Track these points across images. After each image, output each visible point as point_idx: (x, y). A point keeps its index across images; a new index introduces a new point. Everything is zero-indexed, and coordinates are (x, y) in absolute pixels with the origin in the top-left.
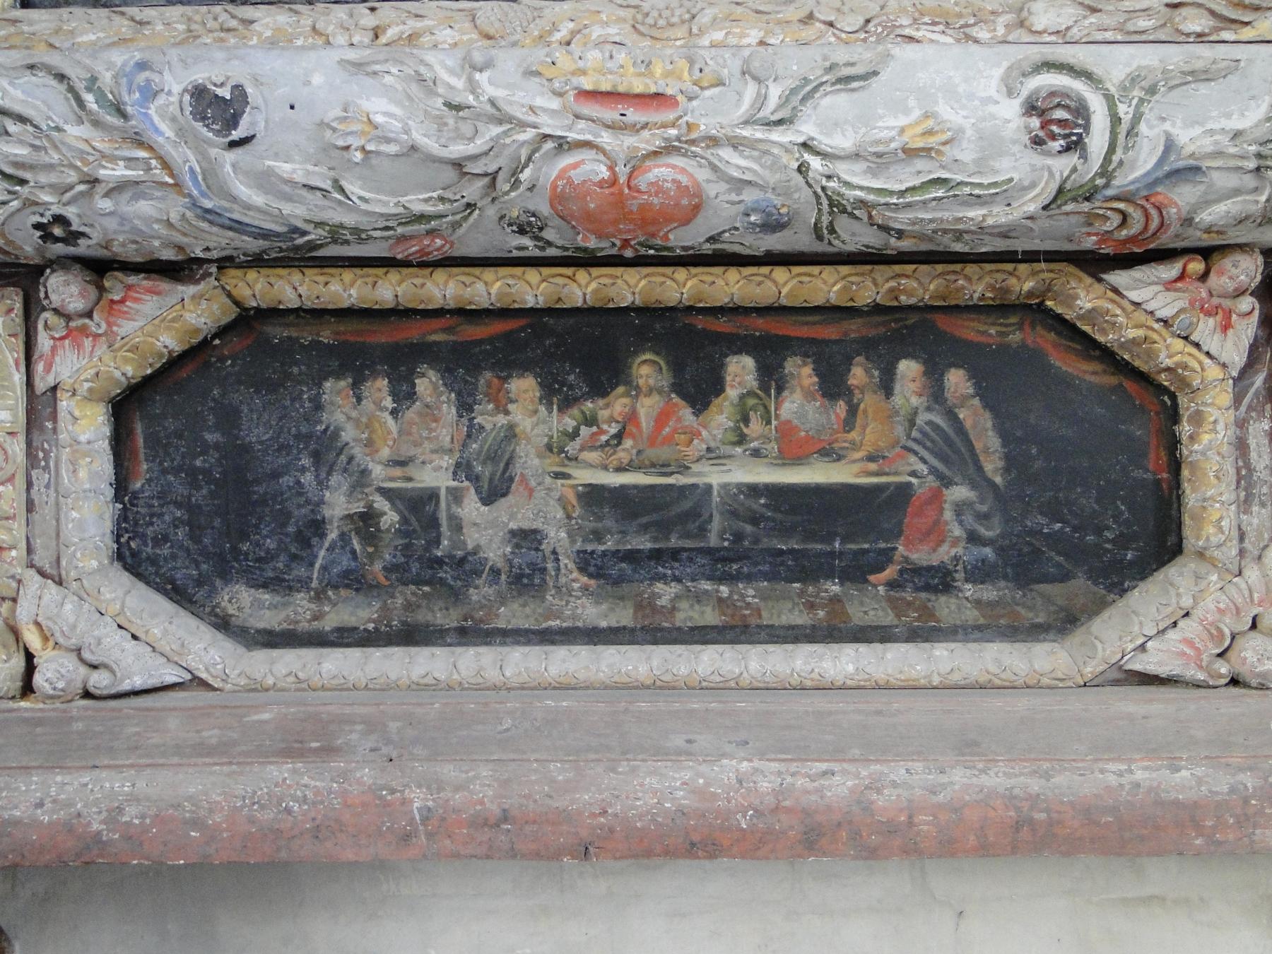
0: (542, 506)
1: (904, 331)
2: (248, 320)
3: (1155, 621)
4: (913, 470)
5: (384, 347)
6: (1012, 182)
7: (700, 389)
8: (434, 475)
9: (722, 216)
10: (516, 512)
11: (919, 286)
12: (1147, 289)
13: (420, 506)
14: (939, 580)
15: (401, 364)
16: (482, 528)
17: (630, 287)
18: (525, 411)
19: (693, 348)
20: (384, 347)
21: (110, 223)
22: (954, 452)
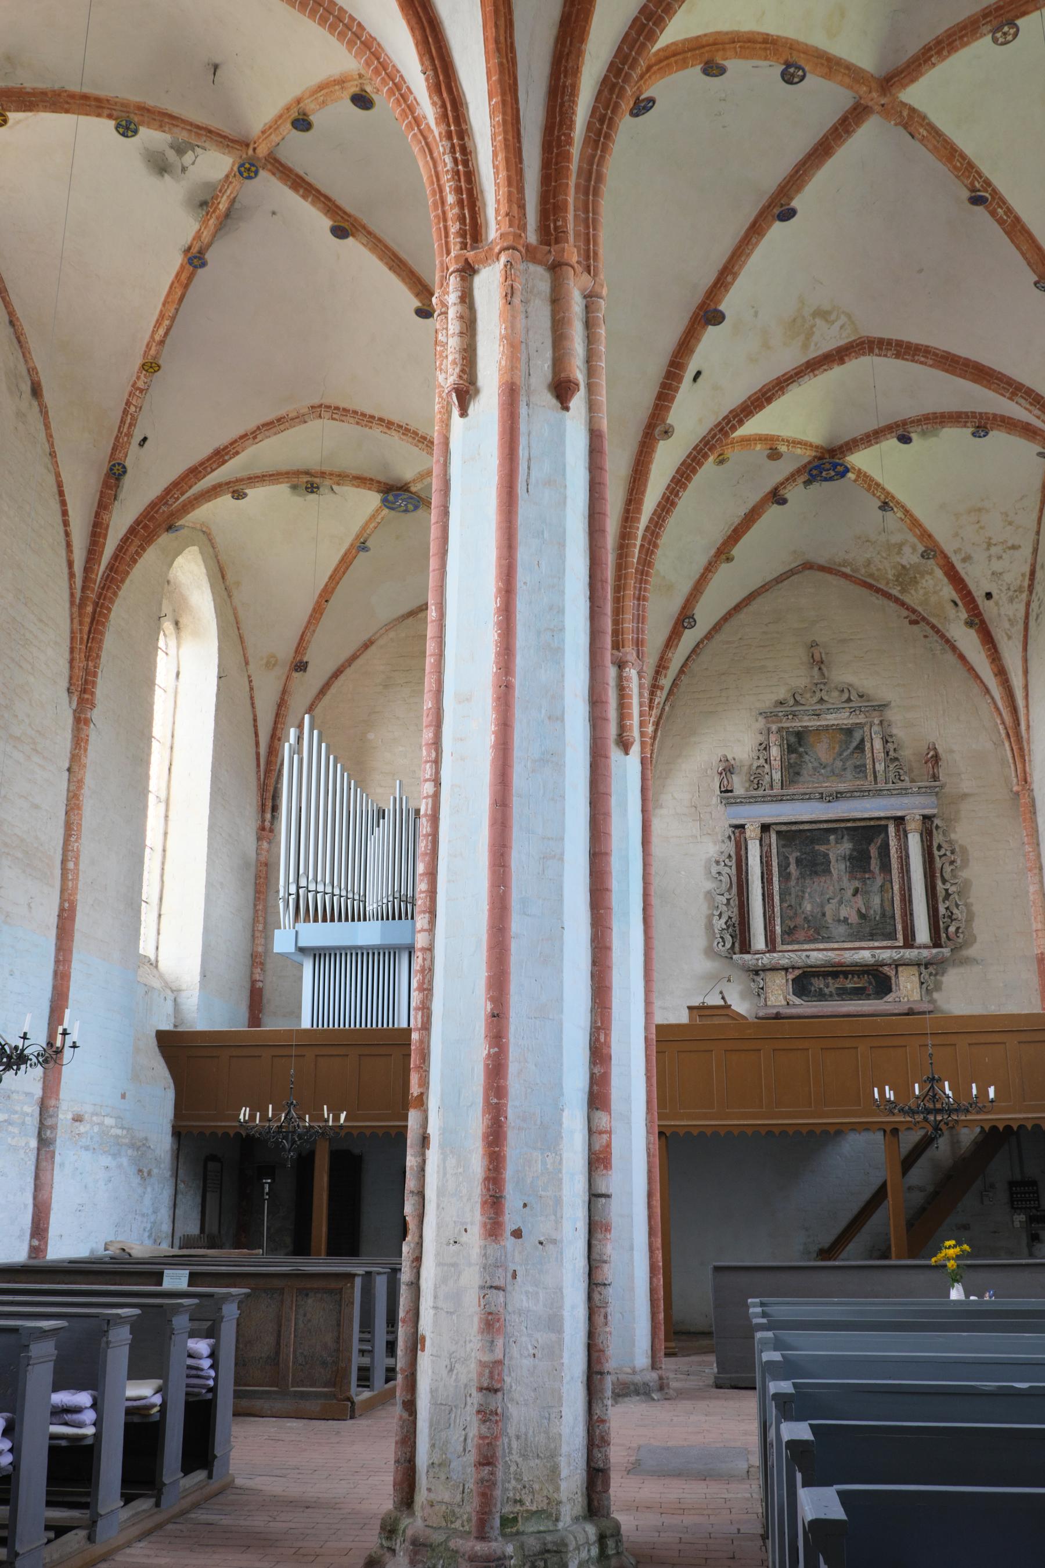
0: (832, 989)
1: (864, 972)
2: (804, 972)
3: (889, 998)
4: (867, 985)
5: (817, 974)
6: (872, 961)
7: (847, 978)
8: (822, 986)
9: (848, 963)
10: (830, 989)
11: (865, 968)
12: (886, 968)
13: (821, 989)
14: (870, 995)
15: (818, 977)
16: (826, 991)
17: (839, 969)
18: (830, 980)
19: (846, 974)
20: (817, 974)
21: (796, 965)
22: (870, 983)
